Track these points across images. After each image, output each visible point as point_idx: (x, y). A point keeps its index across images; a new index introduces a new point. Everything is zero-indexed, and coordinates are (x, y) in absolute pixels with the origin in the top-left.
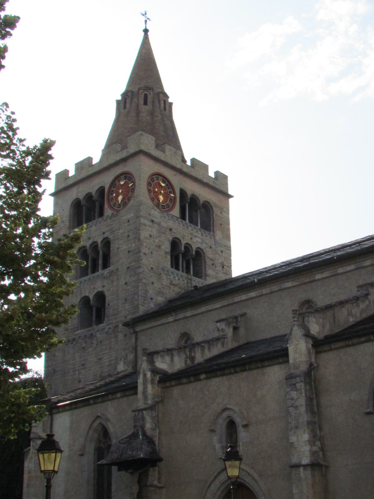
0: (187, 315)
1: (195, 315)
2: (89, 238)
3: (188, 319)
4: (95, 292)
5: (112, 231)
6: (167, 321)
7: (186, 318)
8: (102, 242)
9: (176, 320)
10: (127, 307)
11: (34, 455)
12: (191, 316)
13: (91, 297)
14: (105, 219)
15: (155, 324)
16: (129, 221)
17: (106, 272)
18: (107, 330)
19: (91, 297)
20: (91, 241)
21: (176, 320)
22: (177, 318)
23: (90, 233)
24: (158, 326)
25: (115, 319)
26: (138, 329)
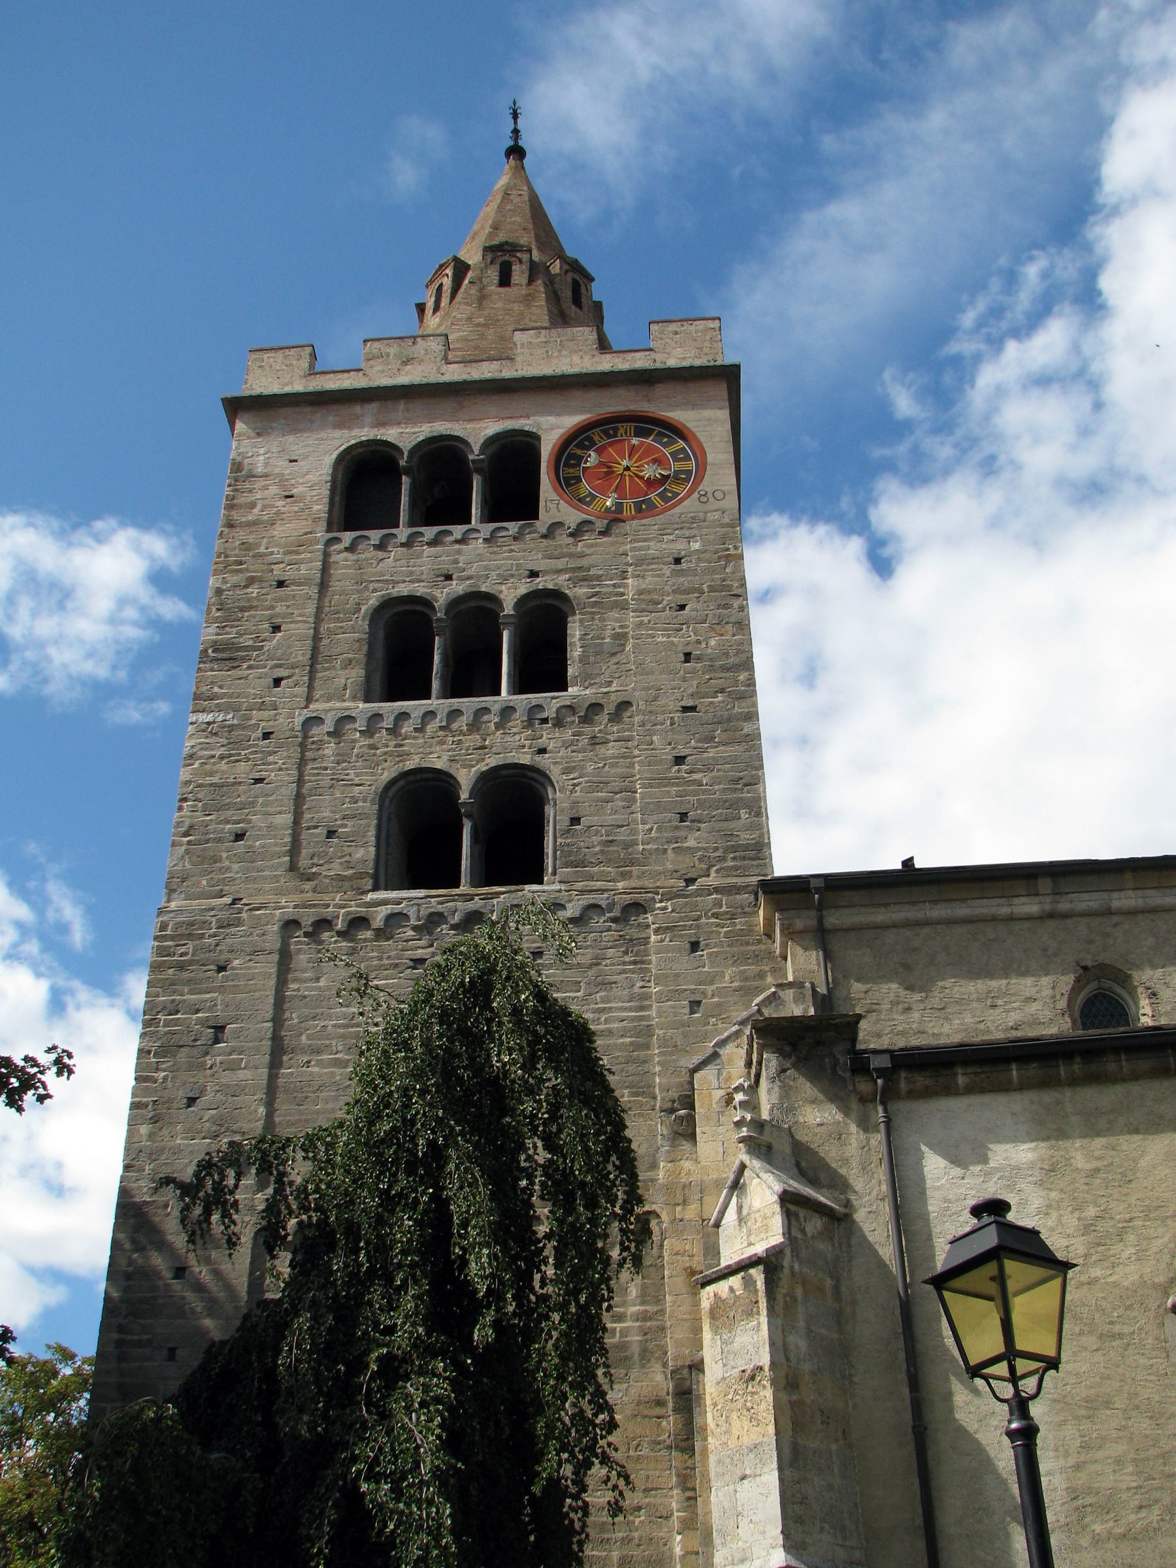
0: (1115, 904)
1: (1155, 910)
2: (449, 577)
3: (1115, 919)
4: (492, 761)
5: (582, 576)
6: (1004, 911)
7: (1108, 912)
8: (522, 601)
9: (1052, 915)
10: (691, 843)
11: (799, 1292)
12: (1132, 913)
13: (466, 779)
14: (544, 531)
15: (961, 911)
16: (678, 561)
17: (555, 704)
18: (571, 911)
19: (466, 779)
20: (457, 588)
21: (1052, 915)
22: (1064, 906)
23: (456, 562)
24: (951, 922)
25: (624, 876)
26: (833, 919)
